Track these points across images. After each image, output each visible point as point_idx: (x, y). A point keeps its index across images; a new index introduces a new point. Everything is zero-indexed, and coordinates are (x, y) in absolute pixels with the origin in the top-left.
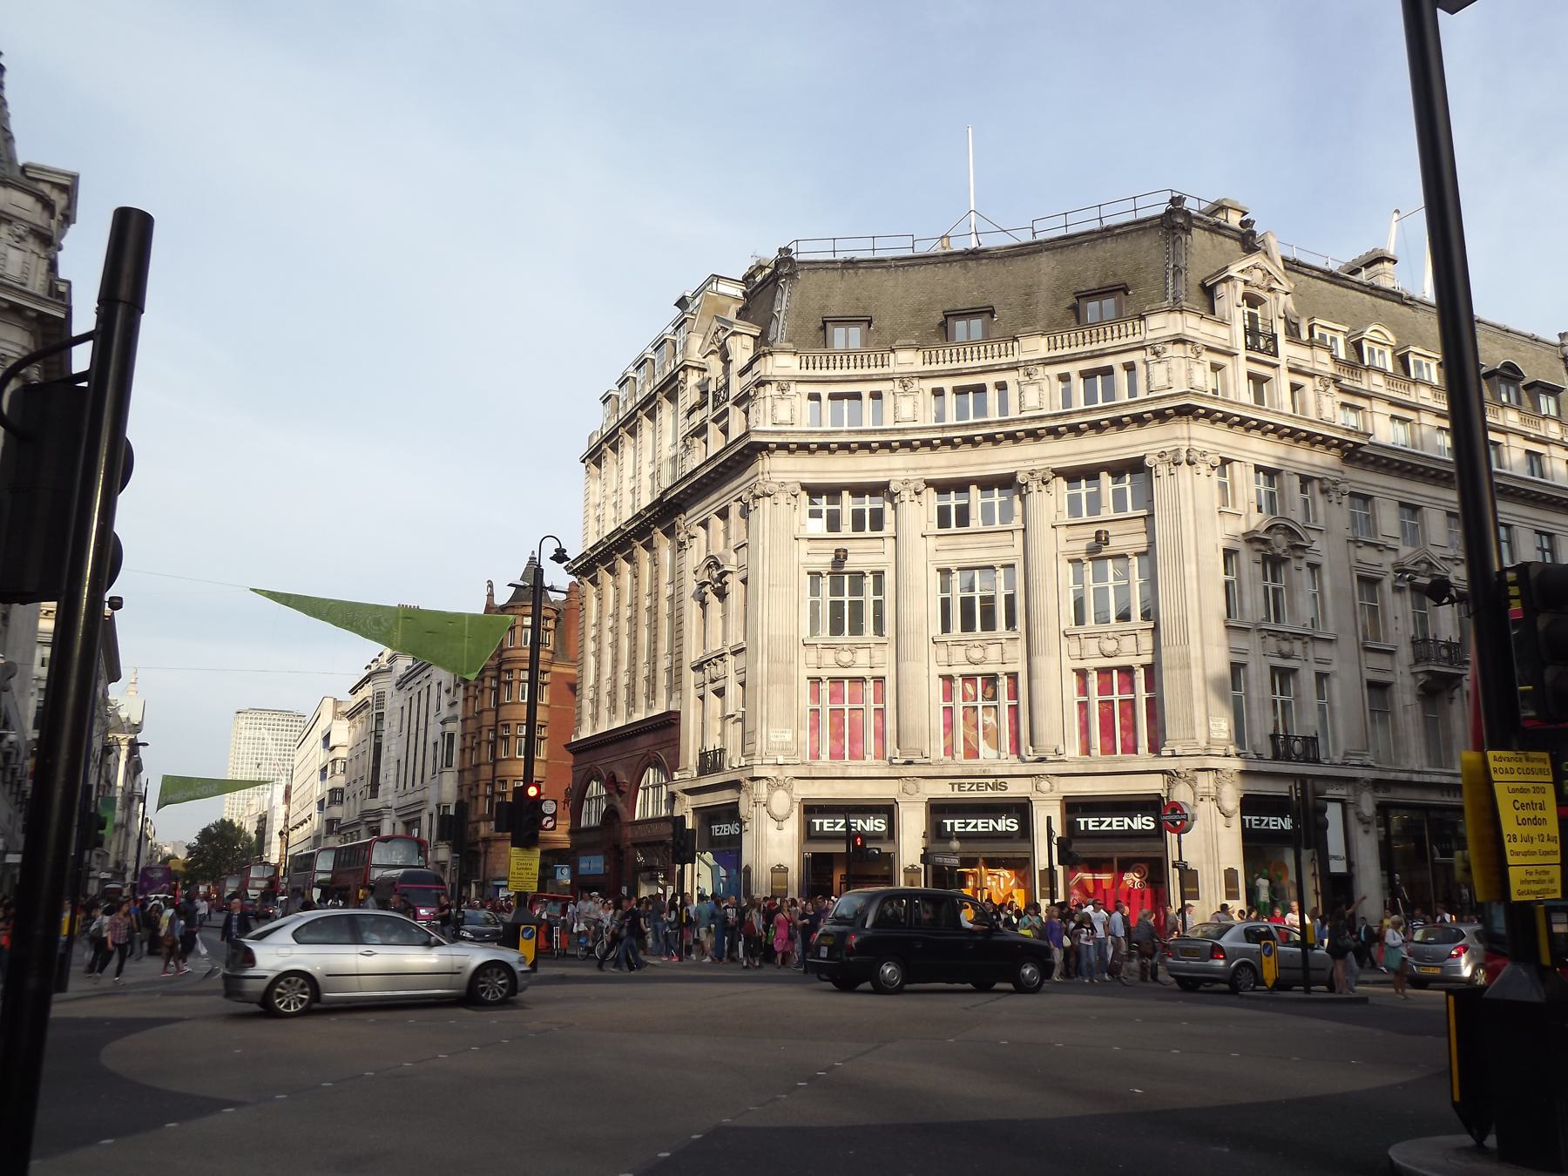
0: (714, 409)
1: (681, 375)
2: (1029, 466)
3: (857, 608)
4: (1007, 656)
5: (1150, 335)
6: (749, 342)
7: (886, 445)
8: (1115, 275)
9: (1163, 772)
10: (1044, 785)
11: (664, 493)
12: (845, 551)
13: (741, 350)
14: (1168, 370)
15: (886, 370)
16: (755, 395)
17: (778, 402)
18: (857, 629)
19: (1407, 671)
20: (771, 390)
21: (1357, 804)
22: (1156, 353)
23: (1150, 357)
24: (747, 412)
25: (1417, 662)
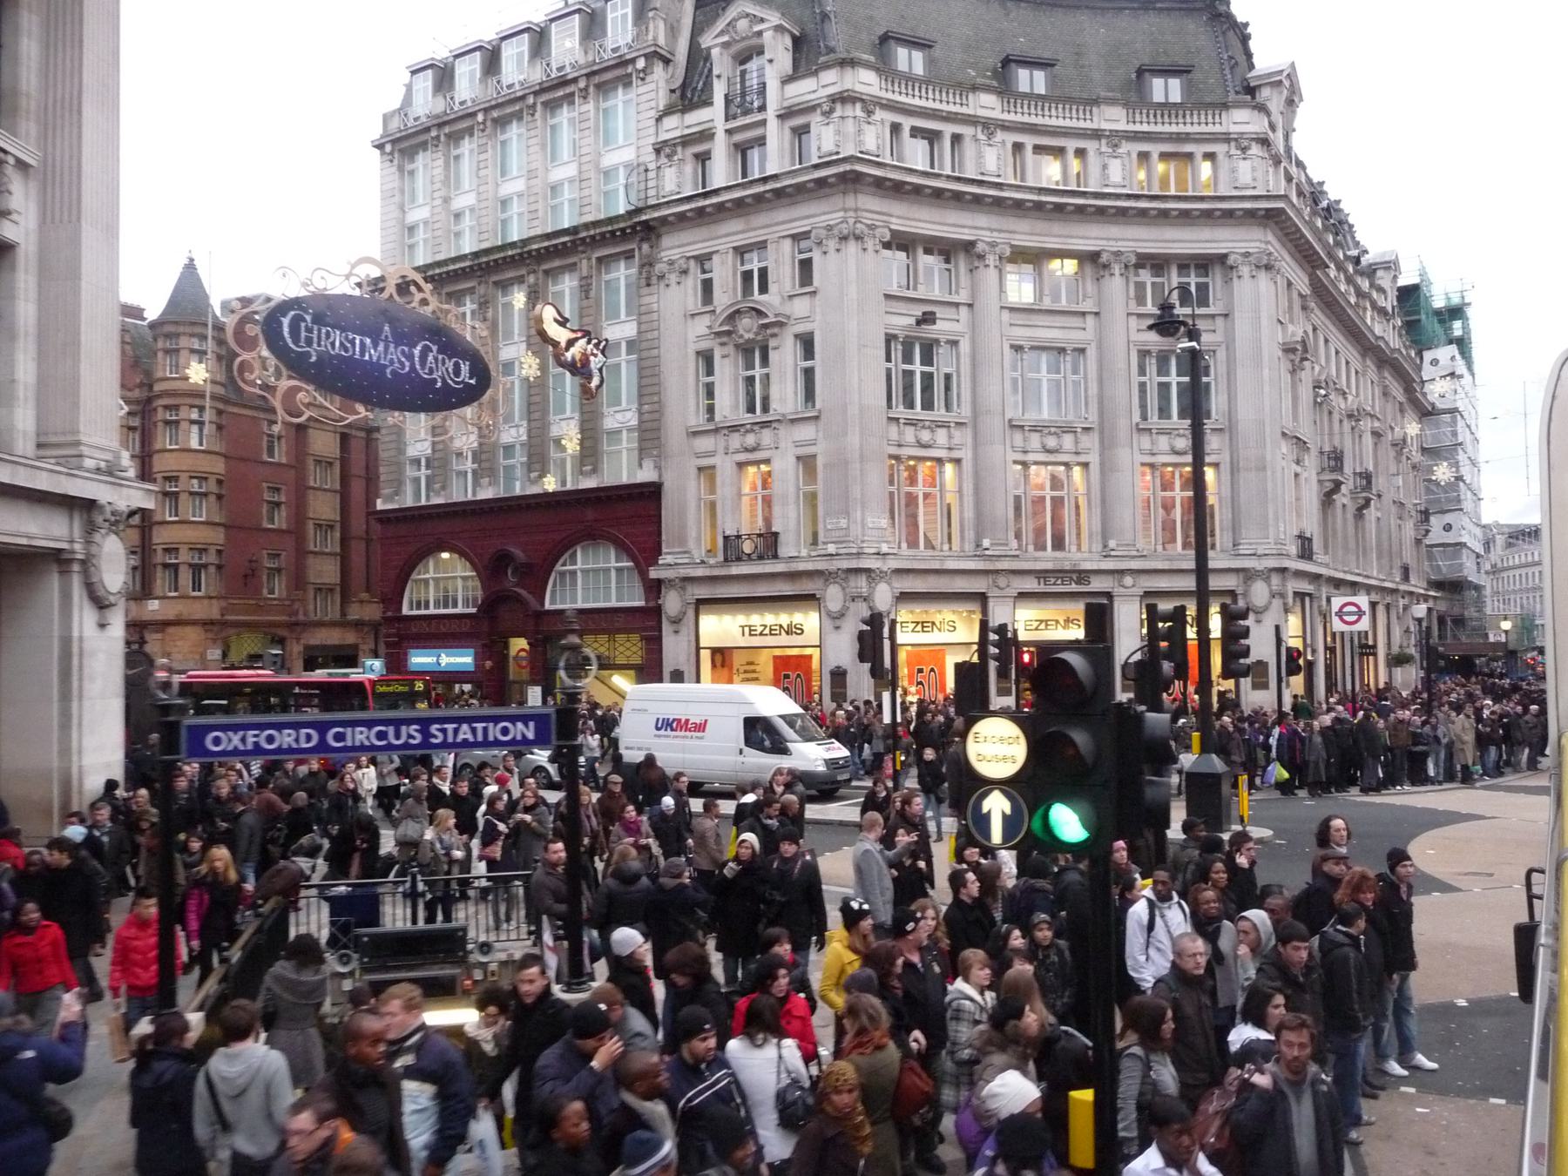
0: (728, 117)
1: (641, 64)
2: (1114, 246)
3: (928, 379)
4: (1081, 446)
5: (1234, 129)
6: (788, 41)
7: (977, 200)
8: (1165, 52)
9: (1237, 571)
10: (1128, 580)
11: (638, 211)
12: (933, 313)
13: (779, 53)
14: (1254, 169)
15: (964, 110)
16: (828, 114)
17: (865, 127)
18: (928, 405)
19: (1314, 478)
20: (858, 110)
21: (1320, 598)
22: (1244, 150)
23: (1233, 151)
24: (801, 132)
25: (1323, 469)
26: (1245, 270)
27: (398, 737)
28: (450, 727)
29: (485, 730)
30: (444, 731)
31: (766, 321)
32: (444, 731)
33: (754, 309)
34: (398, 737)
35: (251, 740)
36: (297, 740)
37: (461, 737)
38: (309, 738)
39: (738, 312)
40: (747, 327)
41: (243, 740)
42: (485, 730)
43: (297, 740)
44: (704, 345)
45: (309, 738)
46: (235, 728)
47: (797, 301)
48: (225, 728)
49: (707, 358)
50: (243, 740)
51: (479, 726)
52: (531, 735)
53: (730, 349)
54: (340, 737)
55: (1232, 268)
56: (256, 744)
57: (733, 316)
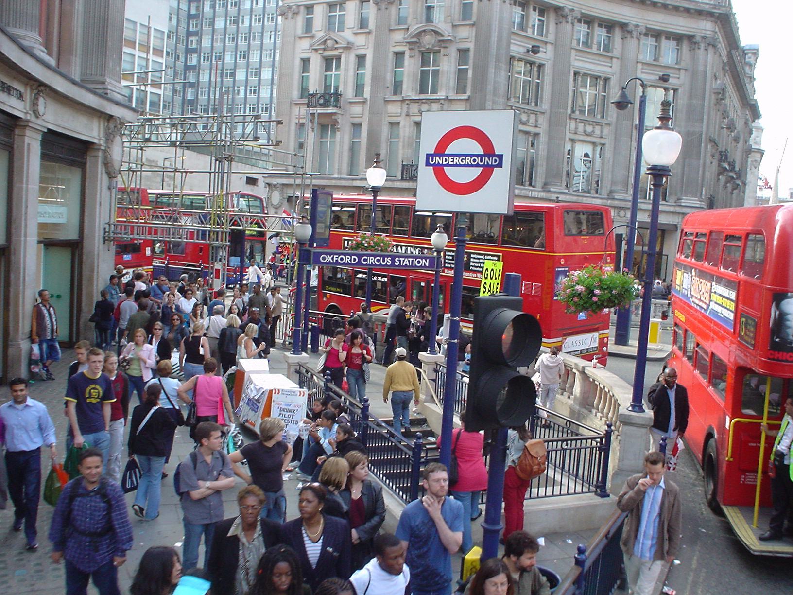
26: (702, 46)
27: (384, 262)
28: (402, 259)
29: (412, 261)
30: (400, 261)
31: (442, 38)
32: (400, 261)
33: (432, 30)
34: (384, 262)
35: (335, 259)
36: (351, 260)
37: (405, 263)
38: (355, 260)
39: (424, 31)
40: (428, 41)
41: (333, 259)
42: (412, 261)
43: (351, 260)
44: (399, 49)
45: (355, 260)
46: (330, 254)
47: (460, 29)
48: (327, 254)
49: (399, 56)
50: (333, 259)
51: (411, 260)
52: (427, 265)
53: (416, 53)
54: (365, 260)
55: (695, 43)
56: (337, 261)
57: (419, 34)
